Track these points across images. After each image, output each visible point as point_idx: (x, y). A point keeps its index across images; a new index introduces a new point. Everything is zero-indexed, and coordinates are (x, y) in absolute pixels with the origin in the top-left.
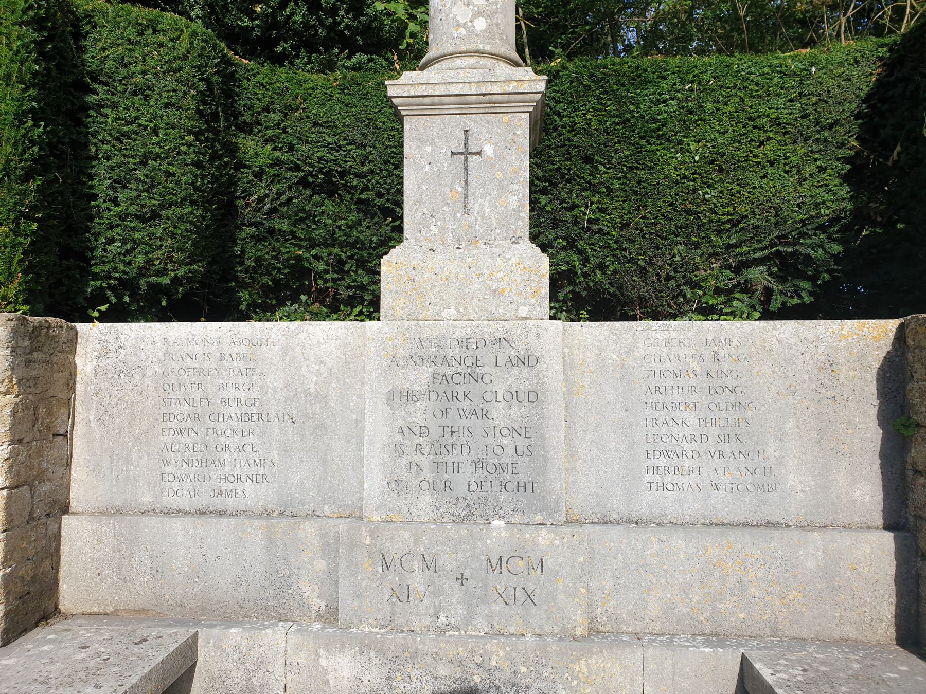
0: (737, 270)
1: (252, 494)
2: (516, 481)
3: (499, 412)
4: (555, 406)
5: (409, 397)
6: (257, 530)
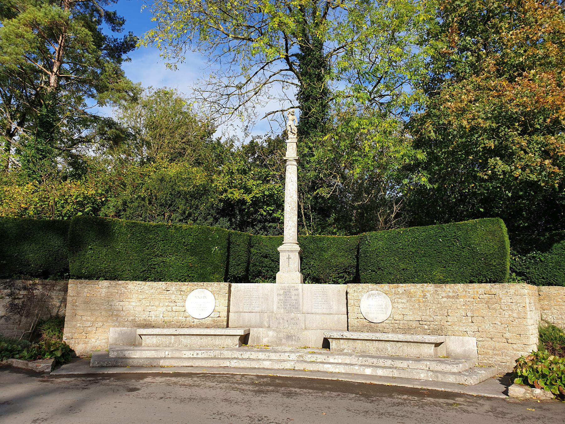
0: (338, 274)
1: (257, 309)
2: (296, 307)
3: (293, 297)
4: (301, 297)
5: (280, 295)
6: (258, 314)
